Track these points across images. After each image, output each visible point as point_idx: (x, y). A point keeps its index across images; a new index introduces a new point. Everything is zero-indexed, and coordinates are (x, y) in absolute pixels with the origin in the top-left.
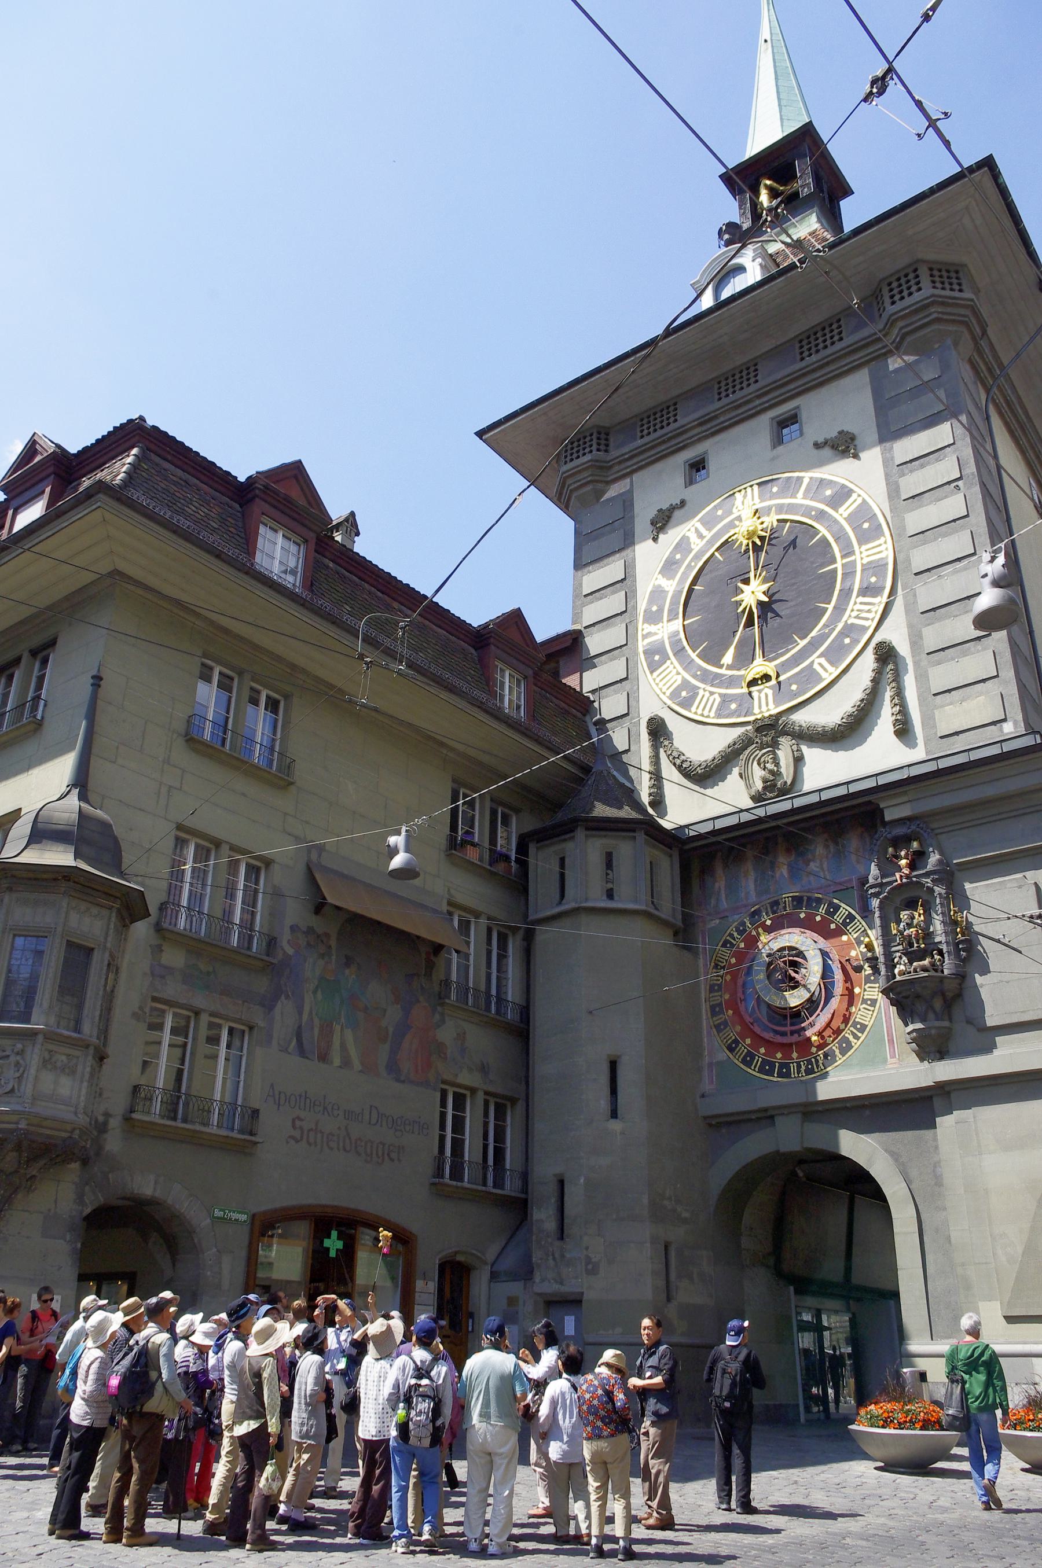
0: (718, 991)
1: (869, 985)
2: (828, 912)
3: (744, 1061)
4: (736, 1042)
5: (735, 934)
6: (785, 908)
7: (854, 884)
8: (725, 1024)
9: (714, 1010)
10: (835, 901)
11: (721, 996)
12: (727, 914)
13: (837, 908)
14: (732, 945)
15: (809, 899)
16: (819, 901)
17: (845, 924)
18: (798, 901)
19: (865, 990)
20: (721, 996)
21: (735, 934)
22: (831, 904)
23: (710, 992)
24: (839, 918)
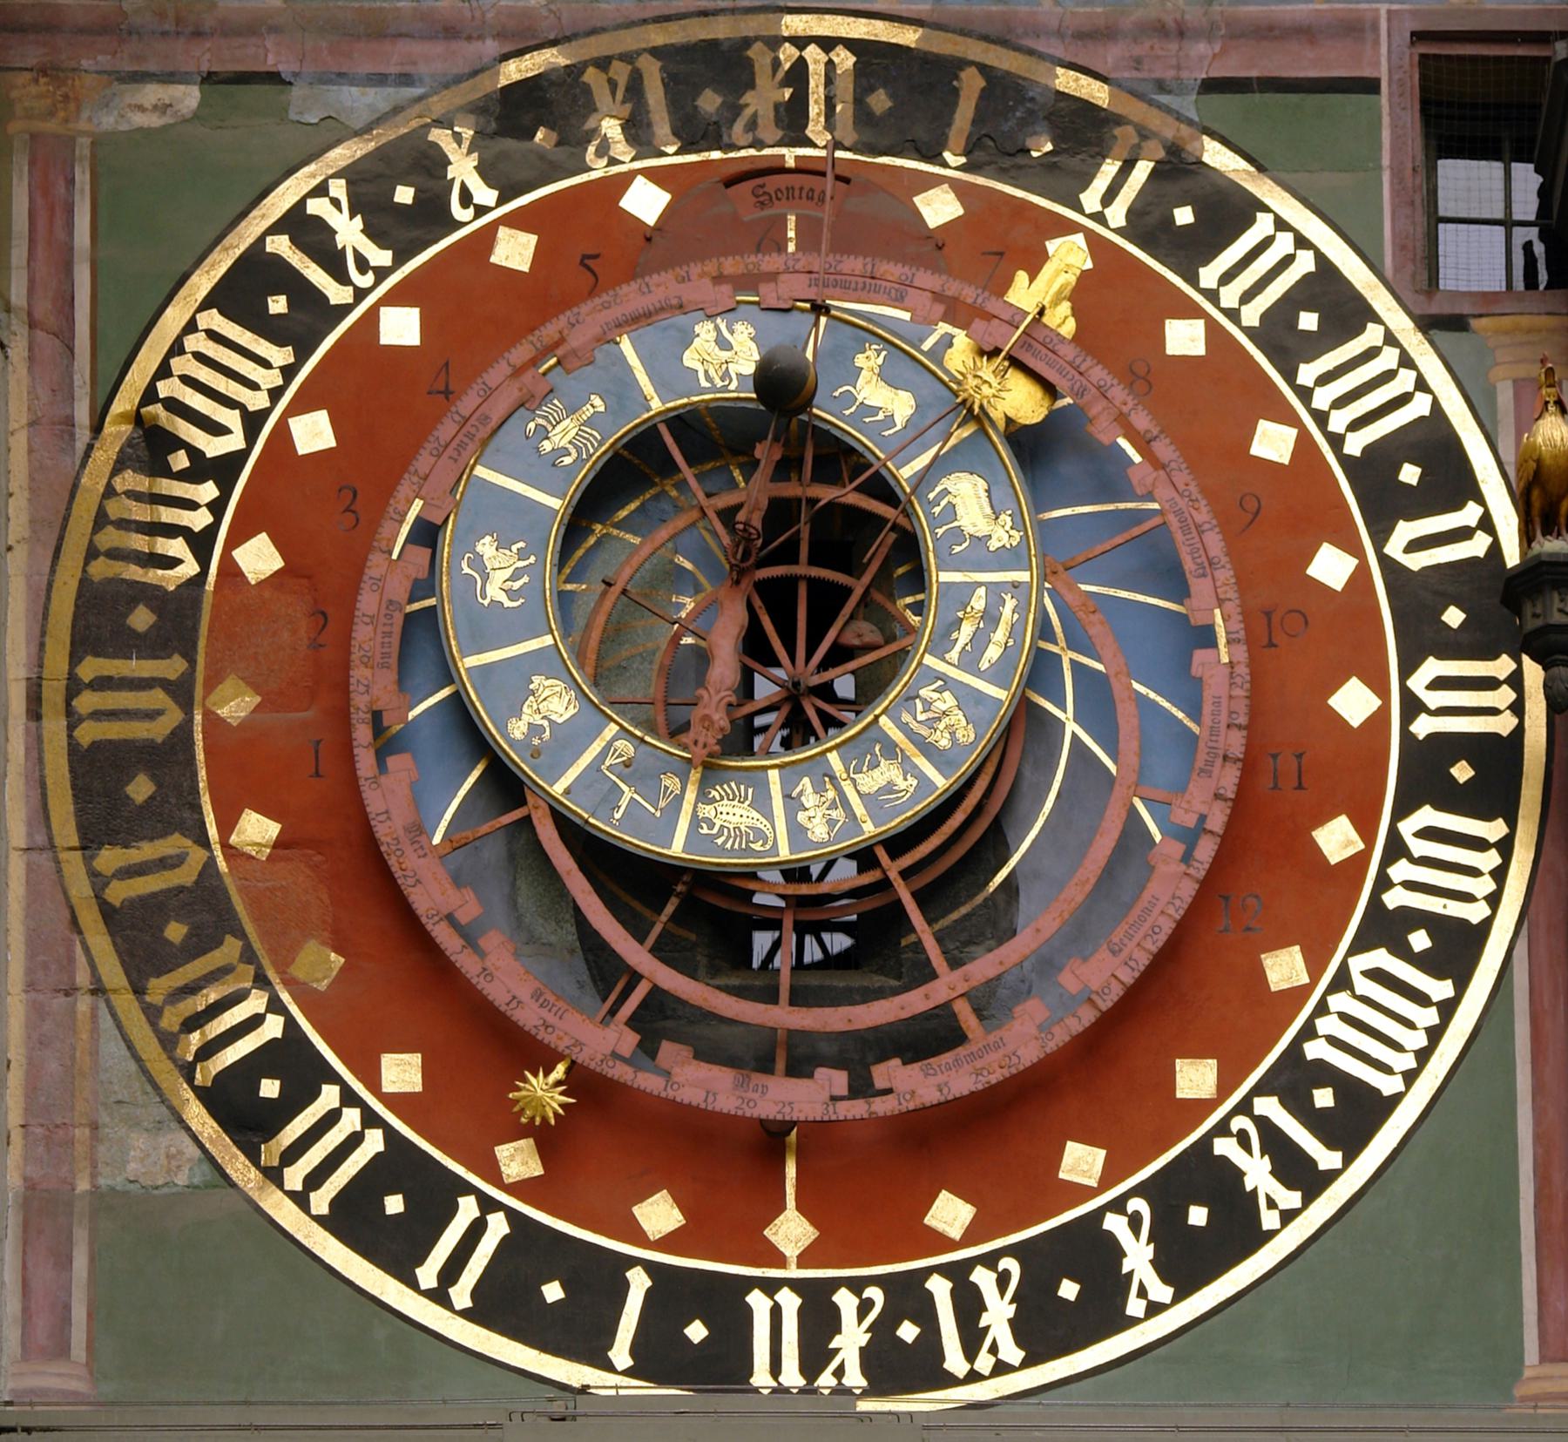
0: (154, 645)
1: (1427, 816)
2: (1148, 224)
3: (353, 1218)
4: (297, 1067)
5: (349, 232)
6: (793, 122)
7: (1387, 60)
8: (208, 909)
9: (116, 791)
10: (1217, 156)
11: (181, 692)
12: (274, 58)
13: (1228, 213)
14: (313, 314)
15: (1003, 92)
16: (1084, 132)
17: (1279, 335)
18: (907, 95)
19: (1396, 849)
20: (181, 692)
21: (349, 232)
22: (1177, 170)
23: (82, 645)
24: (1240, 286)
